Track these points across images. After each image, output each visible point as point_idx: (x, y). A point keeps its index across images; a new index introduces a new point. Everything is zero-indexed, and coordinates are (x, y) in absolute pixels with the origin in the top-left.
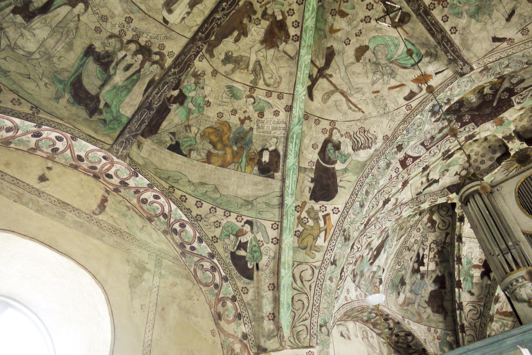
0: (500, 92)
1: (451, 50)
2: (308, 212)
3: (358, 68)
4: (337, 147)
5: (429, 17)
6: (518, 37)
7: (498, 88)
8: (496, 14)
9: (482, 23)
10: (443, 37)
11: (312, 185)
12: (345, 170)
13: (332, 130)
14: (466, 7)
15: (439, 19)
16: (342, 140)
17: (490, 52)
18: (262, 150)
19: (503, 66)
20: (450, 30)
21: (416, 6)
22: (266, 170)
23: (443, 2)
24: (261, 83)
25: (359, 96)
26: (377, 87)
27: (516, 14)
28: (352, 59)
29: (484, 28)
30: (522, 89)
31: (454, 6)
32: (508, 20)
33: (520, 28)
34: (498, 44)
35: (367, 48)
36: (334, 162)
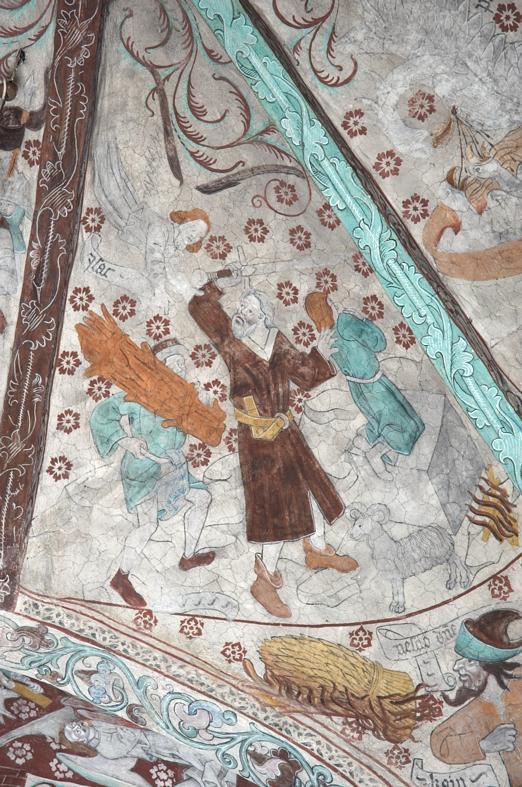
0: (17, 733)
1: (10, 505)
5: (38, 380)
6: (168, 625)
7: (24, 716)
8: (174, 524)
9: (131, 517)
10: (22, 458)
14: (134, 445)
15: (57, 405)
17: (85, 602)
19: (80, 666)
20: (54, 461)
21: (36, 323)
23: (101, 379)
27: (210, 567)
29: (121, 532)
30: (69, 775)
31: (112, 415)
32: (185, 564)
33: (190, 608)
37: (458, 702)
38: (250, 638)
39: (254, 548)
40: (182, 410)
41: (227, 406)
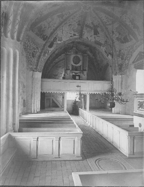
3: (68, 27)
4: (56, 39)
12: (55, 44)
22: (44, 39)
26: (68, 32)
32: (91, 36)
36: (54, 42)
38: (94, 41)
39: (94, 36)
40: (90, 27)
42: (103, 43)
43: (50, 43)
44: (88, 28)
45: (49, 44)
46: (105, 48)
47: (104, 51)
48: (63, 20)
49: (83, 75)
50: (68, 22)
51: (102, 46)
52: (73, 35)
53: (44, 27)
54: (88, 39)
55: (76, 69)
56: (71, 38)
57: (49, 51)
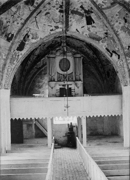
2: (15, 53)
3: (44, 17)
4: (28, 37)
11: (18, 46)
12: (28, 44)
13: (29, 31)
16: (30, 35)
18: (10, 33)
22: (9, 40)
24: (18, 13)
25: (40, 24)
26: (46, 24)
28: (44, 15)
32: (82, 27)
34: (77, 31)
35: (49, 13)
36: (26, 41)
37: (104, 38)
38: (87, 33)
39: (87, 26)
40: (80, 14)
41: (84, 13)
42: (102, 36)
43: (19, 44)
44: (77, 16)
45: (17, 45)
46: (105, 44)
47: (105, 48)
48: (34, 8)
49: (76, 88)
50: (43, 10)
51: (101, 41)
52: (54, 28)
53: (6, 22)
54: (78, 31)
55: (65, 78)
56: (52, 32)
57: (18, 55)
